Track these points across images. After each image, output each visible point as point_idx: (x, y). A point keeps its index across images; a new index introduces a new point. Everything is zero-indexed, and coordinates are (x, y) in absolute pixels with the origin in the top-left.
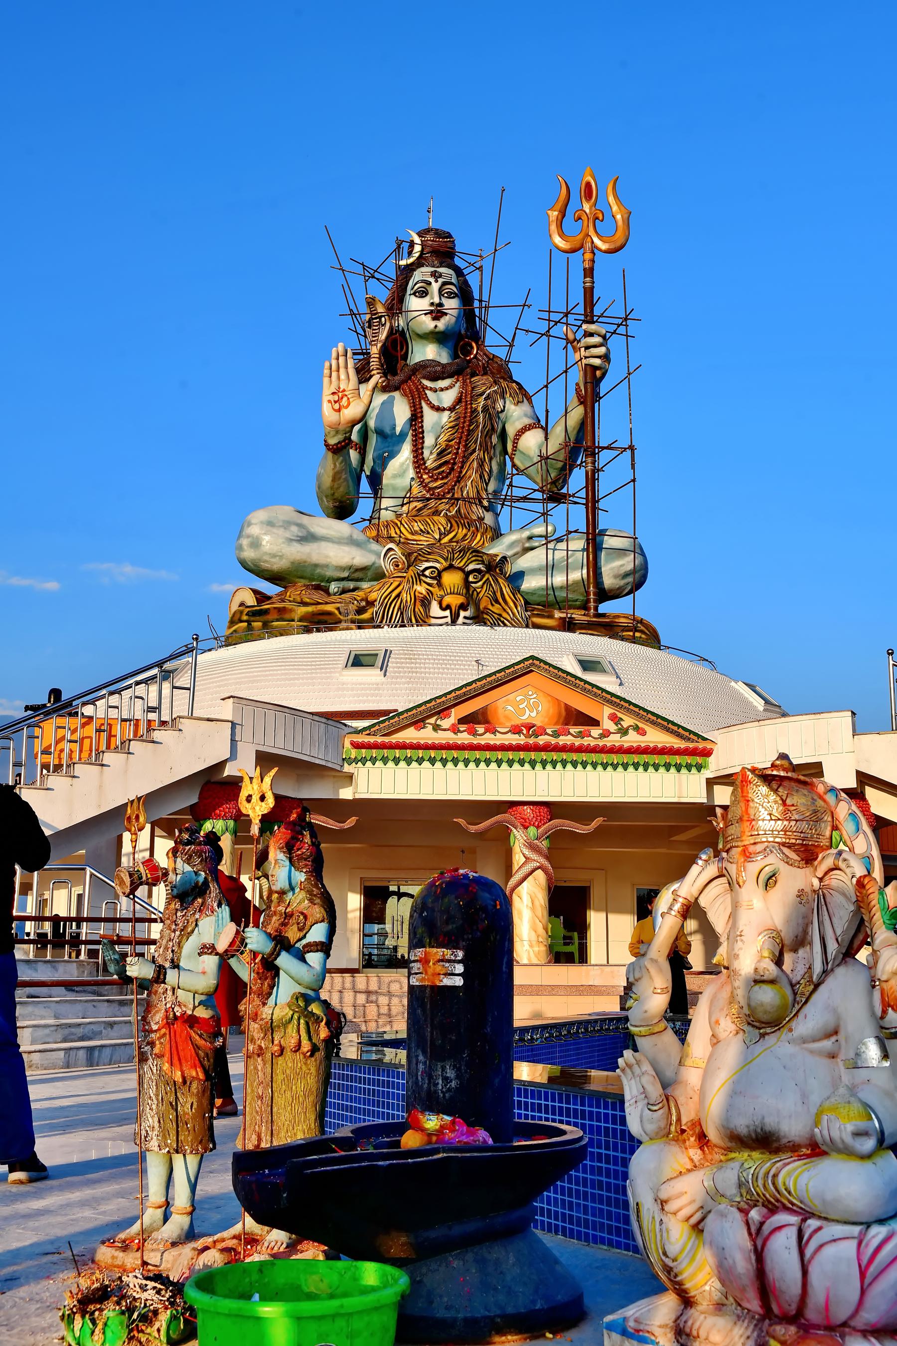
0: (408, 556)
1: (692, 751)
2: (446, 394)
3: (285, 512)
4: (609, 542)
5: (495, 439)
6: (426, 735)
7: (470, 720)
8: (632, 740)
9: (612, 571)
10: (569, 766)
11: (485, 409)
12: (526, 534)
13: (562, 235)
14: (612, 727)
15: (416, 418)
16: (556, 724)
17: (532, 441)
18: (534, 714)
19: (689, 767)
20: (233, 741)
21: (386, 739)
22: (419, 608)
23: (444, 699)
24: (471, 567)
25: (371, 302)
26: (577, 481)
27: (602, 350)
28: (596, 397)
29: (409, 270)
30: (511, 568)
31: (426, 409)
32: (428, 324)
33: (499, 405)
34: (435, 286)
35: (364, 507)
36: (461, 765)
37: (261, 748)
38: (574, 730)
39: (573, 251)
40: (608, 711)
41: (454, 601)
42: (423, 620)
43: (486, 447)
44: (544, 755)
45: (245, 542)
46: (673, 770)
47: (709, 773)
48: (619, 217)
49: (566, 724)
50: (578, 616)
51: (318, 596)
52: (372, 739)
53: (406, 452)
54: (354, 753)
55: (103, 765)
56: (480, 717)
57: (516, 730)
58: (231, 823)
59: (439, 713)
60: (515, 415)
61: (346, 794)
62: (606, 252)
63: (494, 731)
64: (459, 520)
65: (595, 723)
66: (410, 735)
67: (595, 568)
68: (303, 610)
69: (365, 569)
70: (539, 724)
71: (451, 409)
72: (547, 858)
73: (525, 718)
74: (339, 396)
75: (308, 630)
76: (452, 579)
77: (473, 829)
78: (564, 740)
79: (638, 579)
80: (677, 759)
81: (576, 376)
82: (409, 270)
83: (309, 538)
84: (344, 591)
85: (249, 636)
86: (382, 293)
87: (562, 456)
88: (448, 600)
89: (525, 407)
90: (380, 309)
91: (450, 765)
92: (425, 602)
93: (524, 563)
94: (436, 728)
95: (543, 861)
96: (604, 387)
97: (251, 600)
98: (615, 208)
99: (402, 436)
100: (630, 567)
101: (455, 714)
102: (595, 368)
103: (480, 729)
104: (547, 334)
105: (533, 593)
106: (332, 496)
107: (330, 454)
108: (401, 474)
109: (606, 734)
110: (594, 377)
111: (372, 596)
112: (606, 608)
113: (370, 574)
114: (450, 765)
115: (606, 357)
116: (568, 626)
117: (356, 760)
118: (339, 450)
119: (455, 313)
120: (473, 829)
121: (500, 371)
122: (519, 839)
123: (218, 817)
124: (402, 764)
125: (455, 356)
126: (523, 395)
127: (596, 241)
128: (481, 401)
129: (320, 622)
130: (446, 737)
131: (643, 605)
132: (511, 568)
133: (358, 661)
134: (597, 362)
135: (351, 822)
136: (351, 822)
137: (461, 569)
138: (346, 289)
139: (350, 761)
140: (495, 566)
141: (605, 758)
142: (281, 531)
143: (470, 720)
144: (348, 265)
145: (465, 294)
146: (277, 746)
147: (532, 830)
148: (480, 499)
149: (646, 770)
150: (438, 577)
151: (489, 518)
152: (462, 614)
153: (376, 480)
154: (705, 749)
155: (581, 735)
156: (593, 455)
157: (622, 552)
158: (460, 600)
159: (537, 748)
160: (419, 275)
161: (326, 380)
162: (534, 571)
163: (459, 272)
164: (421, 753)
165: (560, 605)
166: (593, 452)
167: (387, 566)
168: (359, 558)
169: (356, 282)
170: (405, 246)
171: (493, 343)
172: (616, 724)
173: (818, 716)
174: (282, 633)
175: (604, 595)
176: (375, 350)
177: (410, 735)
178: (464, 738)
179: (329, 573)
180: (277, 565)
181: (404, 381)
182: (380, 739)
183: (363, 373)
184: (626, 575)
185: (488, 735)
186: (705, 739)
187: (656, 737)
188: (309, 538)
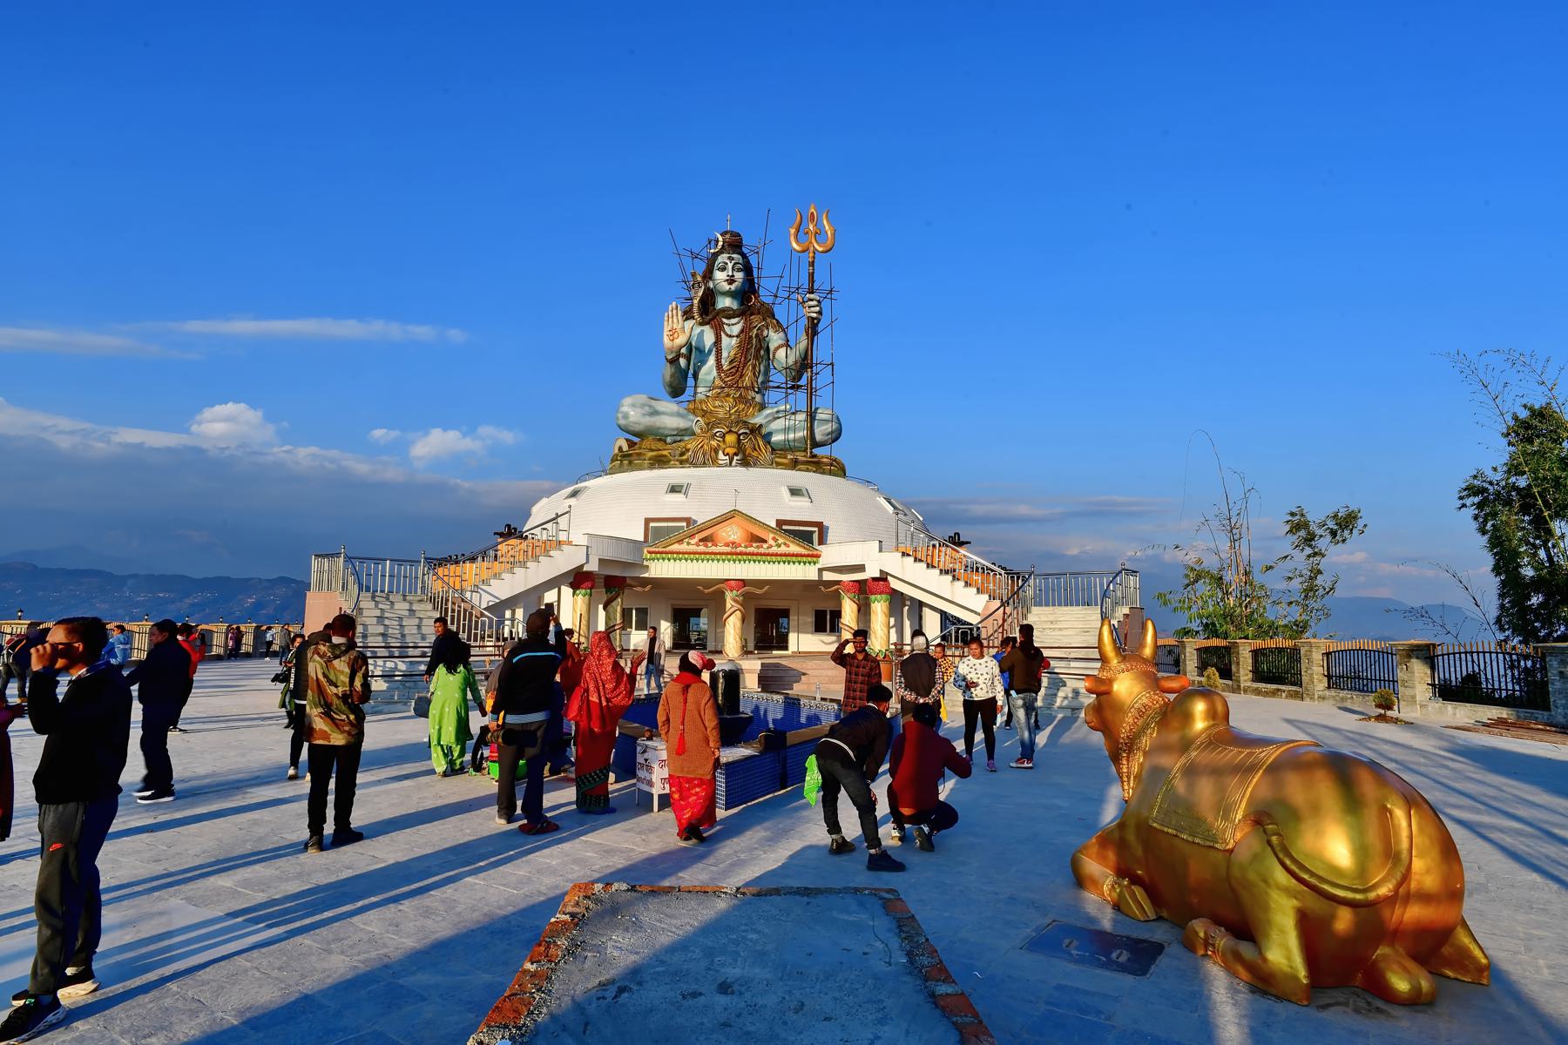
3: (642, 398)
4: (819, 416)
6: (684, 547)
8: (783, 549)
9: (821, 432)
13: (797, 241)
15: (718, 341)
17: (781, 353)
25: (694, 275)
26: (803, 381)
28: (815, 333)
29: (716, 255)
30: (764, 431)
32: (726, 287)
35: (689, 391)
41: (731, 451)
42: (715, 462)
43: (757, 357)
47: (819, 566)
50: (800, 456)
51: (660, 445)
53: (712, 361)
57: (727, 545)
60: (775, 339)
64: (741, 399)
68: (651, 454)
75: (652, 467)
76: (731, 438)
78: (750, 550)
79: (836, 436)
81: (804, 322)
82: (716, 255)
83: (655, 413)
85: (621, 470)
86: (701, 267)
97: (625, 448)
101: (698, 537)
105: (778, 443)
106: (670, 385)
112: (816, 451)
115: (820, 313)
116: (794, 465)
118: (674, 362)
122: (729, 596)
125: (742, 304)
126: (779, 326)
129: (660, 462)
131: (837, 451)
132: (764, 431)
133: (674, 489)
138: (681, 264)
140: (755, 430)
145: (747, 269)
150: (723, 437)
151: (758, 398)
153: (695, 376)
162: (778, 431)
163: (744, 256)
165: (792, 450)
167: (698, 431)
168: (681, 423)
169: (687, 261)
171: (765, 296)
174: (640, 468)
175: (815, 444)
178: (702, 548)
180: (638, 428)
183: (688, 315)
188: (655, 413)
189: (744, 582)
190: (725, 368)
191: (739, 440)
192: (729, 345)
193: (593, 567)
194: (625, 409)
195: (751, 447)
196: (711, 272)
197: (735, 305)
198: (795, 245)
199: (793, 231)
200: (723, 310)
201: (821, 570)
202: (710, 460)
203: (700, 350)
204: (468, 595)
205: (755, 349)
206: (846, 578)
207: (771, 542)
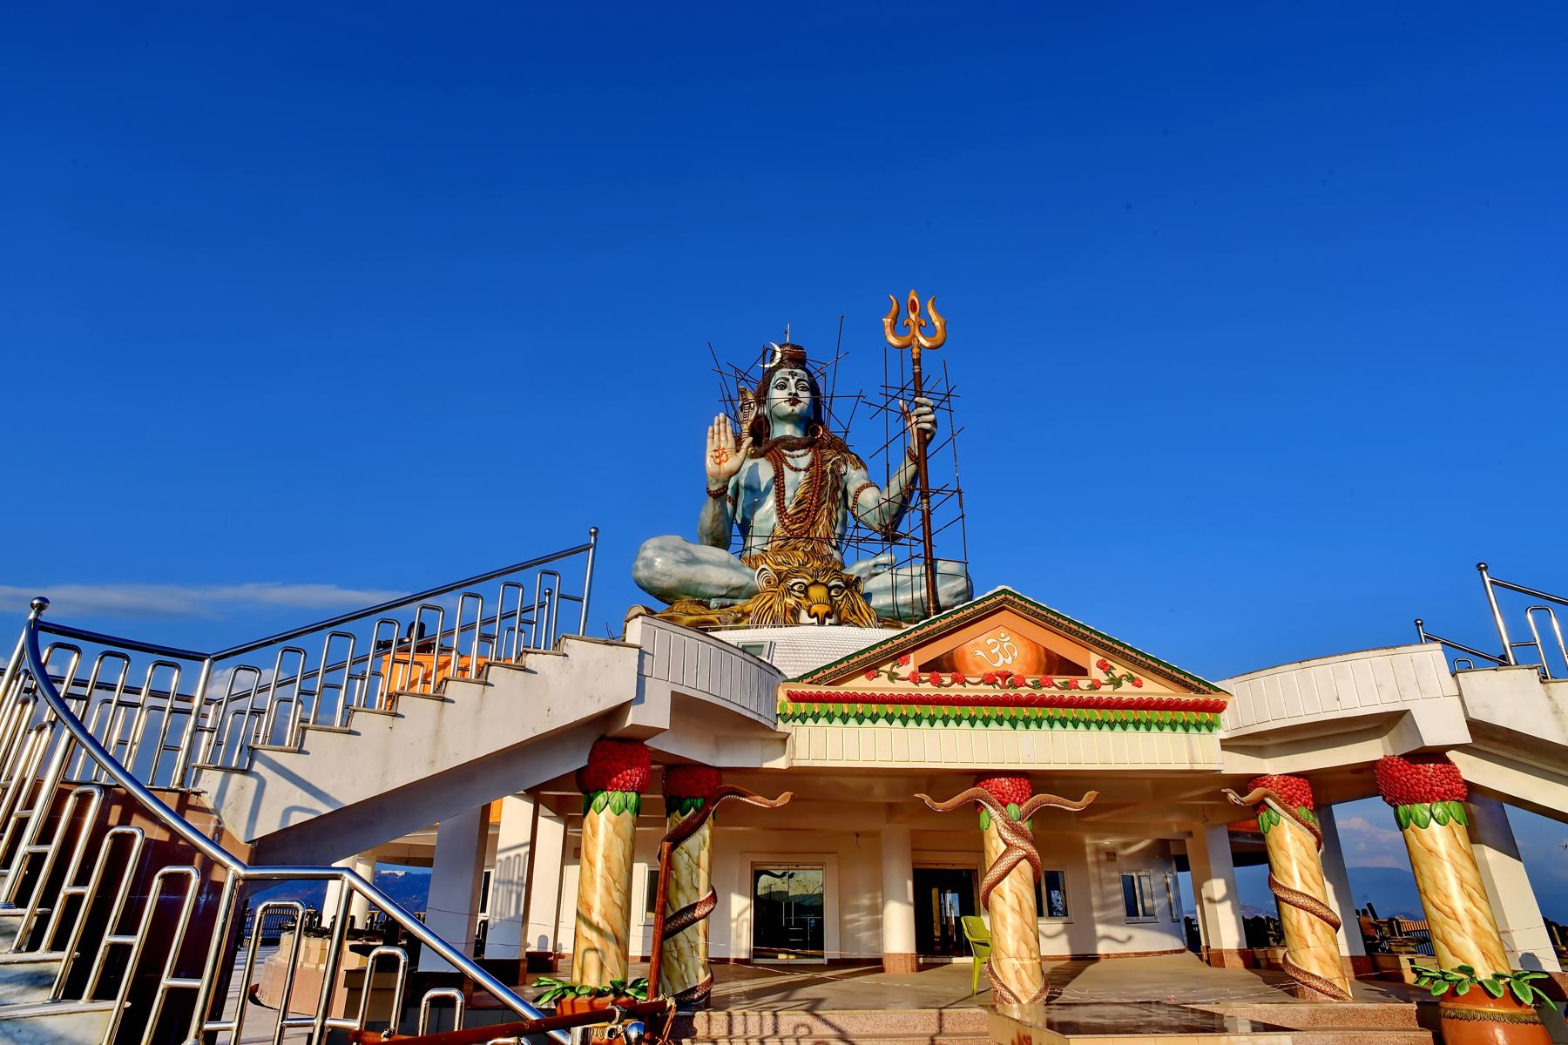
0: (779, 574)
2: (803, 459)
3: (676, 540)
4: (942, 567)
5: (840, 494)
6: (880, 684)
7: (932, 668)
8: (1127, 691)
9: (945, 590)
10: (1057, 725)
11: (832, 471)
12: (872, 562)
14: (1103, 678)
15: (778, 477)
16: (1036, 672)
17: (869, 497)
18: (1009, 661)
19: (1198, 726)
20: (641, 678)
21: (833, 690)
22: (789, 616)
23: (902, 639)
24: (833, 583)
26: (911, 523)
27: (931, 417)
32: (787, 408)
34: (792, 382)
36: (925, 723)
37: (679, 689)
38: (1058, 680)
39: (901, 348)
40: (1094, 658)
41: (822, 609)
43: (833, 499)
45: (640, 563)
46: (1180, 729)
49: (1049, 672)
51: (699, 609)
52: (814, 689)
53: (770, 502)
54: (791, 708)
55: (444, 700)
56: (945, 664)
57: (989, 680)
58: (632, 797)
59: (895, 658)
60: (855, 477)
61: (780, 763)
63: (963, 682)
64: (813, 554)
65: (1083, 672)
66: (860, 685)
68: (689, 619)
69: (740, 588)
70: (1016, 672)
71: (806, 470)
72: (1033, 843)
73: (999, 665)
74: (719, 454)
76: (817, 593)
77: (940, 806)
78: (1049, 692)
80: (1181, 716)
83: (693, 561)
87: (899, 500)
88: (815, 608)
90: (750, 397)
91: (912, 723)
92: (795, 613)
93: (869, 585)
94: (893, 677)
95: (1029, 848)
96: (930, 450)
98: (934, 317)
99: (768, 490)
102: (926, 431)
103: (947, 679)
104: (885, 407)
107: (711, 499)
108: (767, 520)
110: (925, 437)
111: (747, 609)
114: (912, 723)
115: (934, 423)
117: (793, 717)
118: (719, 495)
119: (807, 401)
120: (940, 806)
121: (842, 448)
123: (615, 788)
124: (852, 722)
126: (860, 463)
127: (922, 340)
128: (829, 465)
134: (928, 426)
135: (783, 799)
136: (783, 799)
137: (825, 585)
139: (786, 718)
140: (852, 584)
141: (1096, 714)
143: (932, 668)
145: (813, 389)
146: (700, 687)
147: (1013, 809)
148: (829, 538)
149: (1148, 729)
150: (805, 591)
151: (836, 555)
152: (828, 621)
154: (1217, 702)
155: (1067, 686)
156: (927, 497)
157: (954, 576)
158: (826, 609)
160: (778, 374)
161: (709, 441)
164: (874, 708)
166: (925, 495)
167: (760, 583)
168: (736, 579)
169: (731, 382)
170: (769, 353)
171: (834, 427)
172: (1107, 673)
173: (1392, 651)
176: (746, 427)
177: (860, 685)
178: (927, 689)
179: (710, 591)
180: (666, 583)
181: (769, 451)
183: (738, 441)
185: (956, 685)
187: (1153, 688)
188: (693, 561)
189: (1035, 781)
190: (790, 511)
191: (831, 598)
192: (795, 481)
193: (653, 714)
194: (649, 553)
195: (845, 602)
196: (766, 393)
197: (799, 434)
198: (892, 340)
199: (887, 321)
200: (783, 439)
201: (1226, 745)
202: (792, 617)
204: (209, 782)
205: (827, 490)
206: (1274, 766)
207: (1097, 674)
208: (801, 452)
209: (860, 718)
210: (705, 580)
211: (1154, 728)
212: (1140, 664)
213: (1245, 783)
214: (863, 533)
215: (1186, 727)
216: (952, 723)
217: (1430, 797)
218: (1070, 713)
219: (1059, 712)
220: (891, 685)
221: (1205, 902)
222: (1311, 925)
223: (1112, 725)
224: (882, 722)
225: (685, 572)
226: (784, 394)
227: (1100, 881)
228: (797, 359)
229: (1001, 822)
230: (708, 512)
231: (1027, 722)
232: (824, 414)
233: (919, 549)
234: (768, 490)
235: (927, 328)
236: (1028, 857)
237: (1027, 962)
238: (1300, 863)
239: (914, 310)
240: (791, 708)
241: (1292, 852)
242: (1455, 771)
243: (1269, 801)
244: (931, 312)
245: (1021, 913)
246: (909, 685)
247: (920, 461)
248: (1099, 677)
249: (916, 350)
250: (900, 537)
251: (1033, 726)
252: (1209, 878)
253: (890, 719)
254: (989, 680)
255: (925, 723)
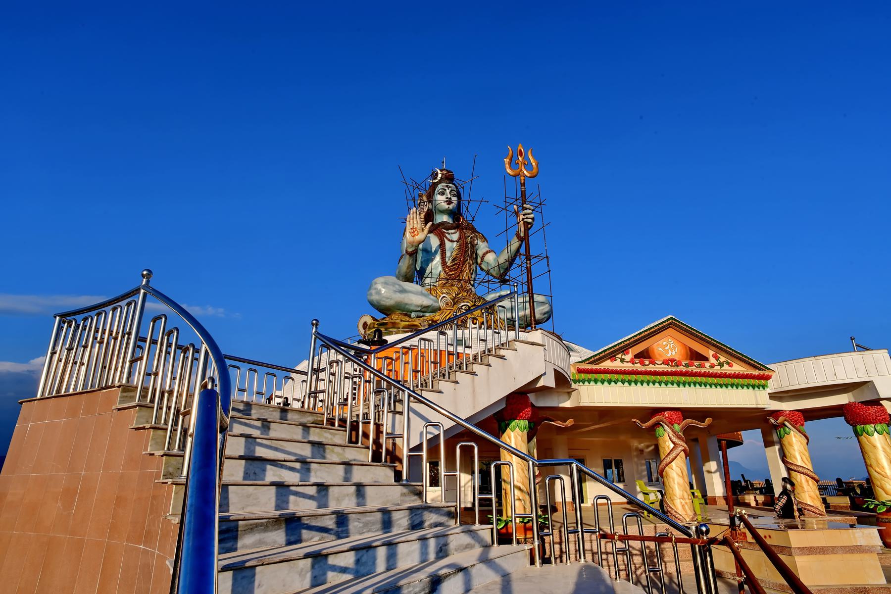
0: (453, 300)
1: (758, 377)
3: (393, 279)
4: (537, 298)
6: (616, 365)
7: (644, 355)
10: (697, 385)
14: (715, 362)
15: (442, 245)
17: (490, 258)
21: (598, 367)
26: (514, 272)
27: (532, 216)
29: (435, 185)
31: (446, 241)
33: (476, 242)
34: (448, 191)
36: (639, 384)
38: (696, 363)
39: (515, 176)
40: (711, 353)
43: (471, 258)
44: (683, 379)
45: (373, 292)
47: (769, 390)
48: (534, 164)
49: (691, 359)
51: (407, 318)
52: (590, 367)
53: (438, 258)
57: (666, 363)
60: (482, 247)
61: (567, 404)
62: (530, 177)
64: (462, 289)
66: (607, 364)
67: (532, 308)
69: (428, 307)
71: (457, 241)
77: (644, 425)
78: (694, 369)
80: (751, 381)
83: (403, 291)
84: (418, 317)
89: (485, 243)
90: (425, 198)
94: (622, 360)
96: (530, 232)
98: (532, 160)
99: (436, 252)
100: (546, 310)
107: (408, 256)
109: (712, 366)
113: (430, 309)
115: (533, 219)
117: (579, 381)
118: (413, 254)
119: (456, 202)
120: (644, 425)
121: (474, 230)
123: (521, 418)
124: (606, 383)
126: (484, 239)
130: (628, 366)
134: (530, 221)
136: (570, 422)
139: (575, 381)
142: (391, 287)
144: (410, 182)
145: (459, 196)
151: (473, 289)
155: (701, 366)
157: (543, 303)
159: (681, 374)
160: (440, 186)
161: (408, 223)
167: (442, 304)
168: (426, 301)
169: (411, 188)
171: (467, 217)
177: (607, 364)
178: (638, 367)
179: (412, 308)
180: (389, 303)
181: (435, 230)
182: (594, 367)
184: (545, 314)
186: (769, 369)
187: (738, 368)
188: (403, 291)
189: (686, 413)
197: (451, 221)
198: (509, 171)
199: (507, 160)
200: (442, 224)
201: (774, 396)
203: (426, 251)
205: (467, 252)
207: (713, 360)
208: (453, 231)
209: (609, 382)
210: (409, 302)
211: (740, 388)
212: (734, 356)
213: (776, 413)
214: (491, 278)
215: (753, 387)
216: (651, 384)
217: (874, 422)
218: (703, 379)
219: (699, 379)
220: (621, 364)
221: (706, 474)
222: (807, 481)
223: (721, 386)
224: (619, 383)
225: (398, 297)
226: (443, 198)
227: (637, 465)
228: (449, 178)
229: (671, 433)
230: (404, 265)
231: (684, 384)
232: (463, 210)
233: (526, 289)
234: (436, 252)
235: (528, 165)
236: (684, 450)
237: (688, 501)
238: (800, 453)
239: (521, 155)
240: (577, 376)
241: (796, 448)
242: (885, 410)
243: (786, 423)
244: (530, 157)
245: (683, 477)
246: (630, 365)
247: (524, 239)
248: (714, 362)
249: (522, 178)
250: (508, 281)
251: (687, 386)
252: (708, 461)
253: (623, 382)
254: (666, 363)
255: (639, 384)
